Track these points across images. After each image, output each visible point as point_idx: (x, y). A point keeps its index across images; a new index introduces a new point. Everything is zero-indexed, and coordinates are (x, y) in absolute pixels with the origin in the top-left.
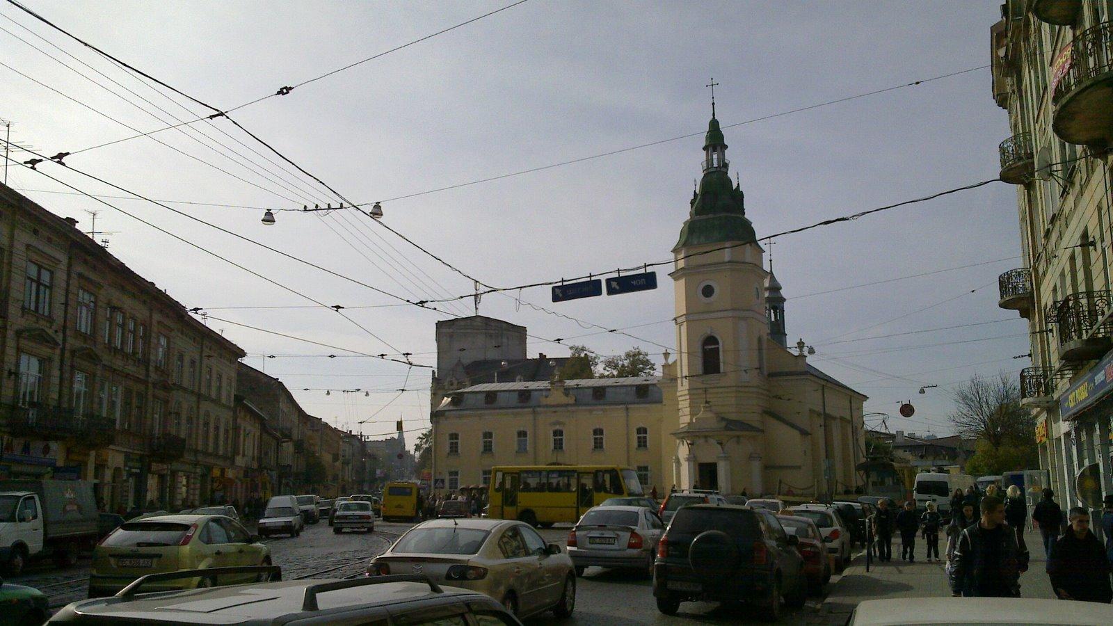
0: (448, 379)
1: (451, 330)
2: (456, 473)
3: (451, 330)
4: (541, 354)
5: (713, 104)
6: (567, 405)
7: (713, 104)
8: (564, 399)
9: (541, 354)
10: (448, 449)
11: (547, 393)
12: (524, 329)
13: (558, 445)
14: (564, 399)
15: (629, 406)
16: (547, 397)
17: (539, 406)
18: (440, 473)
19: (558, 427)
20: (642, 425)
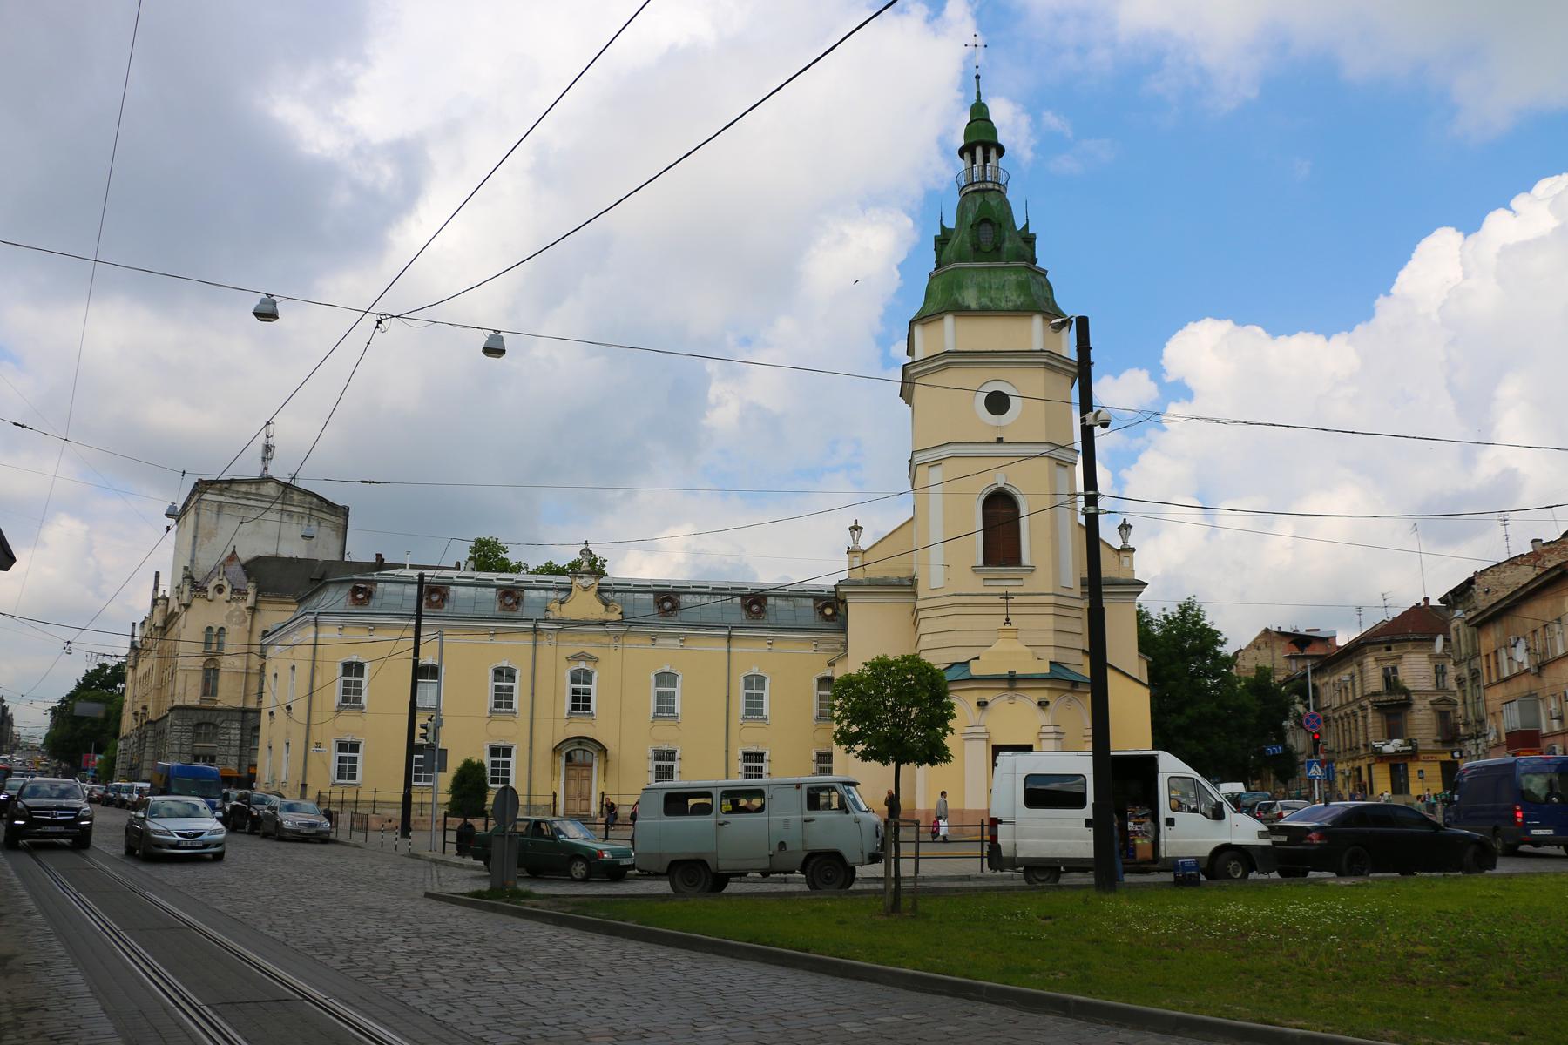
0: (215, 582)
1: (221, 498)
2: (355, 747)
3: (221, 498)
4: (379, 556)
5: (978, 77)
6: (603, 623)
7: (978, 77)
8: (596, 611)
9: (379, 556)
10: (338, 696)
11: (562, 595)
12: (345, 511)
13: (581, 702)
14: (596, 611)
15: (735, 633)
16: (562, 603)
17: (546, 620)
18: (318, 745)
19: (582, 665)
20: (755, 671)
